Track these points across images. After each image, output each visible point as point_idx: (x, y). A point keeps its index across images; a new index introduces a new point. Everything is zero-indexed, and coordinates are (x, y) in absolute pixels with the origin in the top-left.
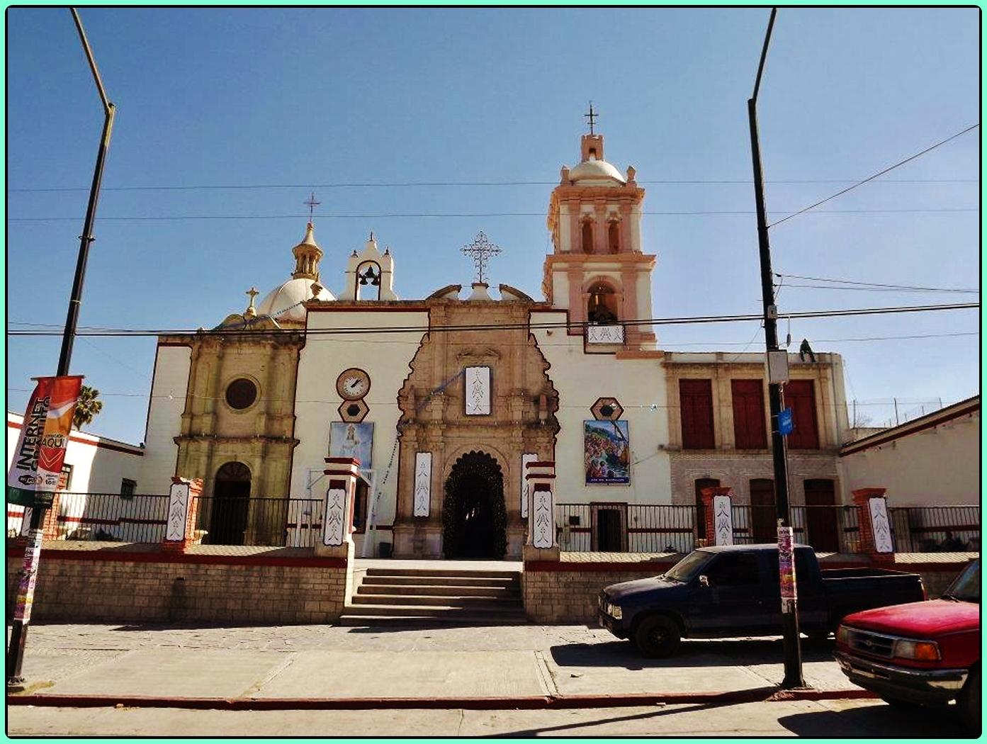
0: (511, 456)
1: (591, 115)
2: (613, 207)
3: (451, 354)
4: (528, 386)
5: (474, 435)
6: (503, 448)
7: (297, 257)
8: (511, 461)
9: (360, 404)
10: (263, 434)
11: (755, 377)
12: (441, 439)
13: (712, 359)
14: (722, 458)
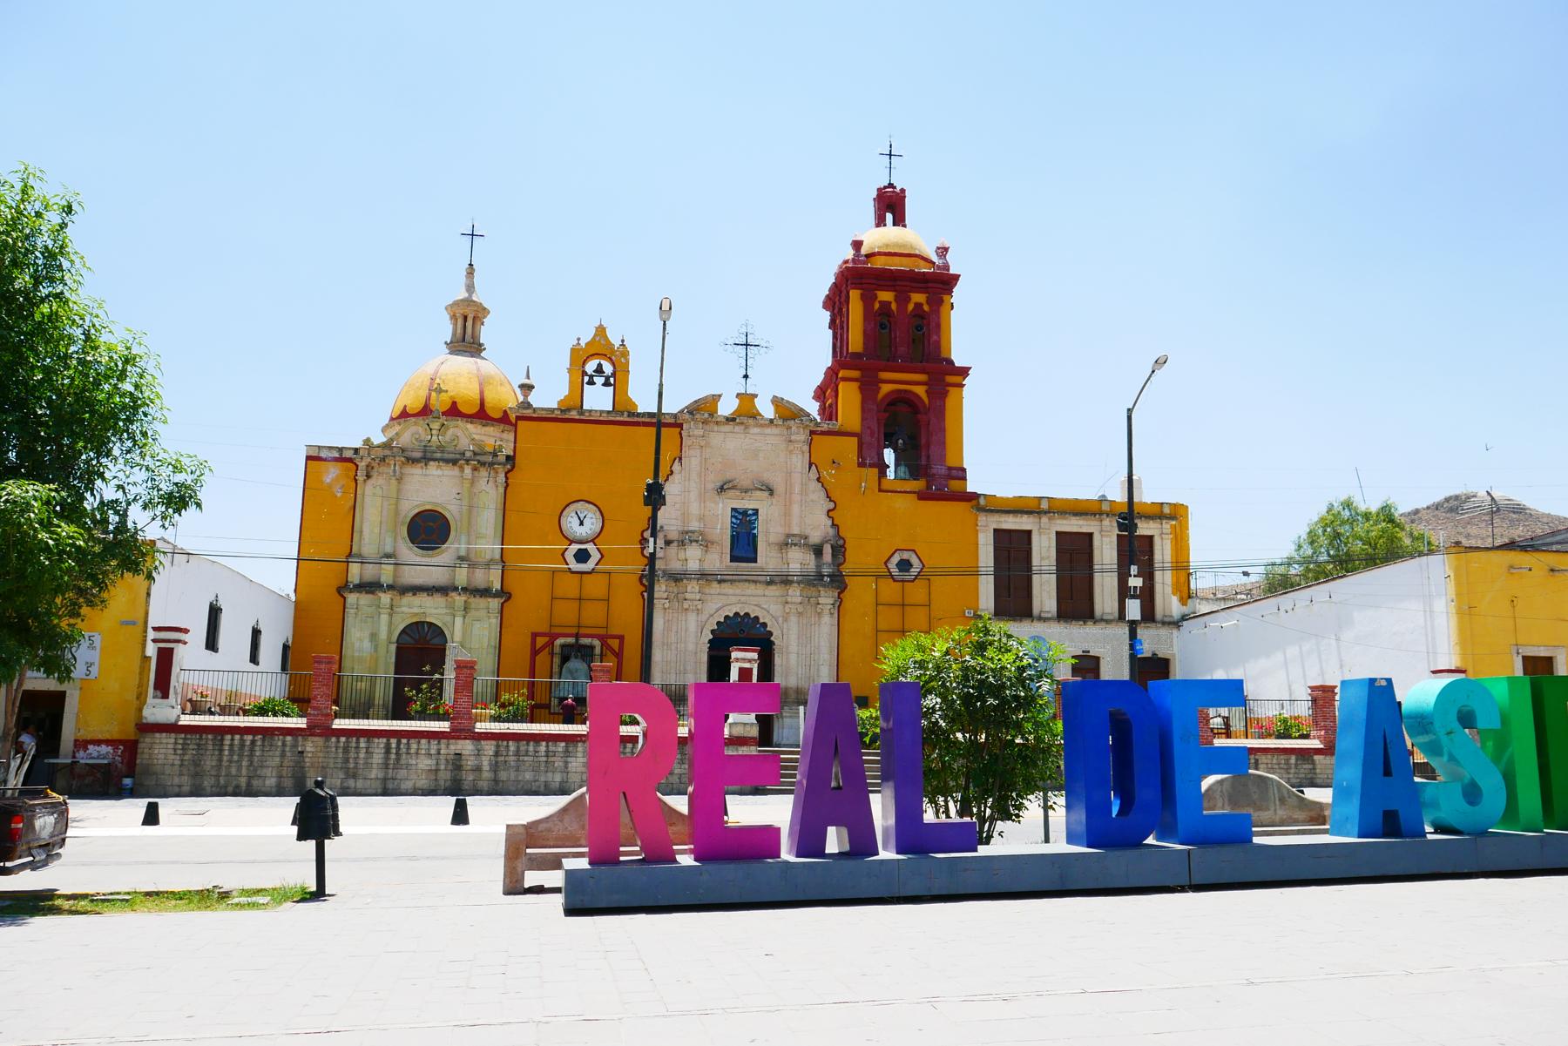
0: (786, 620)
1: (890, 155)
2: (918, 298)
3: (710, 486)
4: (807, 532)
5: (738, 591)
6: (775, 609)
7: (454, 317)
8: (785, 626)
9: (590, 547)
11: (1084, 530)
12: (698, 597)
13: (1033, 505)
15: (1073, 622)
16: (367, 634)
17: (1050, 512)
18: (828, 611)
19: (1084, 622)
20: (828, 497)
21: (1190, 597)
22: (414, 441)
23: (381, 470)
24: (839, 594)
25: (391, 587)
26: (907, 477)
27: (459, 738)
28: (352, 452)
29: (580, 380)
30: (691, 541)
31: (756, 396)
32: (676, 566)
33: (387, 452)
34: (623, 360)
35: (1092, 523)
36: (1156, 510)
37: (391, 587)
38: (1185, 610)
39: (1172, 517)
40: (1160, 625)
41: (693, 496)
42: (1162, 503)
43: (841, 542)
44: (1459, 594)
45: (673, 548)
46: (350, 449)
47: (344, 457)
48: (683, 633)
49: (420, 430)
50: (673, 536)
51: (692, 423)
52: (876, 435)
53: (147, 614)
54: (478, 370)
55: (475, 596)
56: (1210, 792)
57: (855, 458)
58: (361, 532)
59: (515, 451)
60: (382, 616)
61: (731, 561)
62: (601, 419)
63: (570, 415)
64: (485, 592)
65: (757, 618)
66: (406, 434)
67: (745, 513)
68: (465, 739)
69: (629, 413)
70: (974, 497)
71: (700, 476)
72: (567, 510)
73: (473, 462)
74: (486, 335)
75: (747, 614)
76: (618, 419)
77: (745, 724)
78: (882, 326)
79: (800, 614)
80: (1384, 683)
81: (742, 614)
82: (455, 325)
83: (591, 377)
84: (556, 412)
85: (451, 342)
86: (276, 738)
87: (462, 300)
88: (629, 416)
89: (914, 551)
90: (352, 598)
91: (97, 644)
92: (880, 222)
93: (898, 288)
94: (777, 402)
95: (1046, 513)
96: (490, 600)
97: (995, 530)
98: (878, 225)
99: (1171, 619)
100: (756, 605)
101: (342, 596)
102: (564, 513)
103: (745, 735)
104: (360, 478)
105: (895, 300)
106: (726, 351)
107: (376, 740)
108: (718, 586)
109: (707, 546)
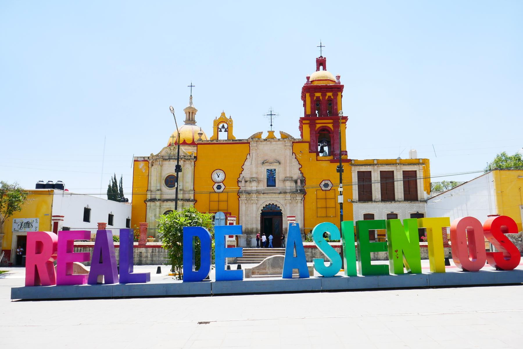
0: (286, 205)
1: (321, 46)
2: (329, 94)
3: (259, 162)
4: (292, 176)
5: (270, 197)
6: (282, 202)
7: (186, 113)
9: (221, 184)
10: (182, 198)
12: (256, 199)
13: (371, 162)
14: (374, 204)
15: (387, 202)
16: (153, 215)
17: (377, 164)
18: (300, 202)
19: (391, 202)
20: (299, 164)
21: (431, 192)
22: (166, 154)
23: (156, 163)
24: (304, 196)
25: (159, 200)
27: (141, 247)
28: (148, 158)
29: (217, 131)
30: (253, 181)
31: (274, 132)
32: (248, 189)
33: (158, 157)
34: (230, 123)
35: (393, 167)
36: (417, 162)
37: (159, 200)
38: (429, 196)
39: (423, 164)
40: (419, 202)
41: (254, 165)
42: (419, 159)
43: (304, 179)
44: (497, 188)
45: (248, 183)
46: (147, 157)
47: (145, 160)
48: (252, 211)
49: (168, 150)
50: (248, 179)
51: (253, 142)
52: (315, 142)
53: (52, 212)
54: (193, 129)
55: (185, 202)
56: (265, 263)
57: (308, 150)
58: (151, 183)
59: (197, 155)
60: (157, 209)
61: (267, 187)
62: (224, 142)
63: (215, 142)
64: (188, 200)
65: (276, 205)
66: (163, 152)
67: (271, 171)
68: (143, 247)
69: (232, 140)
70: (350, 160)
71: (256, 159)
72: (214, 173)
73: (183, 159)
74: (197, 118)
75: (273, 204)
76: (229, 142)
77: (231, 241)
78: (317, 105)
79: (290, 203)
80: (295, 225)
81: (271, 204)
82: (186, 115)
83: (221, 129)
84: (209, 141)
85: (185, 121)
86: (87, 248)
87: (188, 107)
88: (232, 141)
89: (329, 180)
90: (148, 204)
91: (38, 221)
92: (318, 69)
93: (322, 91)
94: (281, 133)
95: (376, 165)
96: (190, 202)
97: (358, 171)
98: (317, 71)
99: (424, 200)
100: (276, 201)
101: (145, 203)
102: (213, 174)
103: (231, 245)
104: (150, 166)
105: (321, 96)
106: (265, 117)
107: (116, 248)
108: (263, 195)
109: (259, 182)
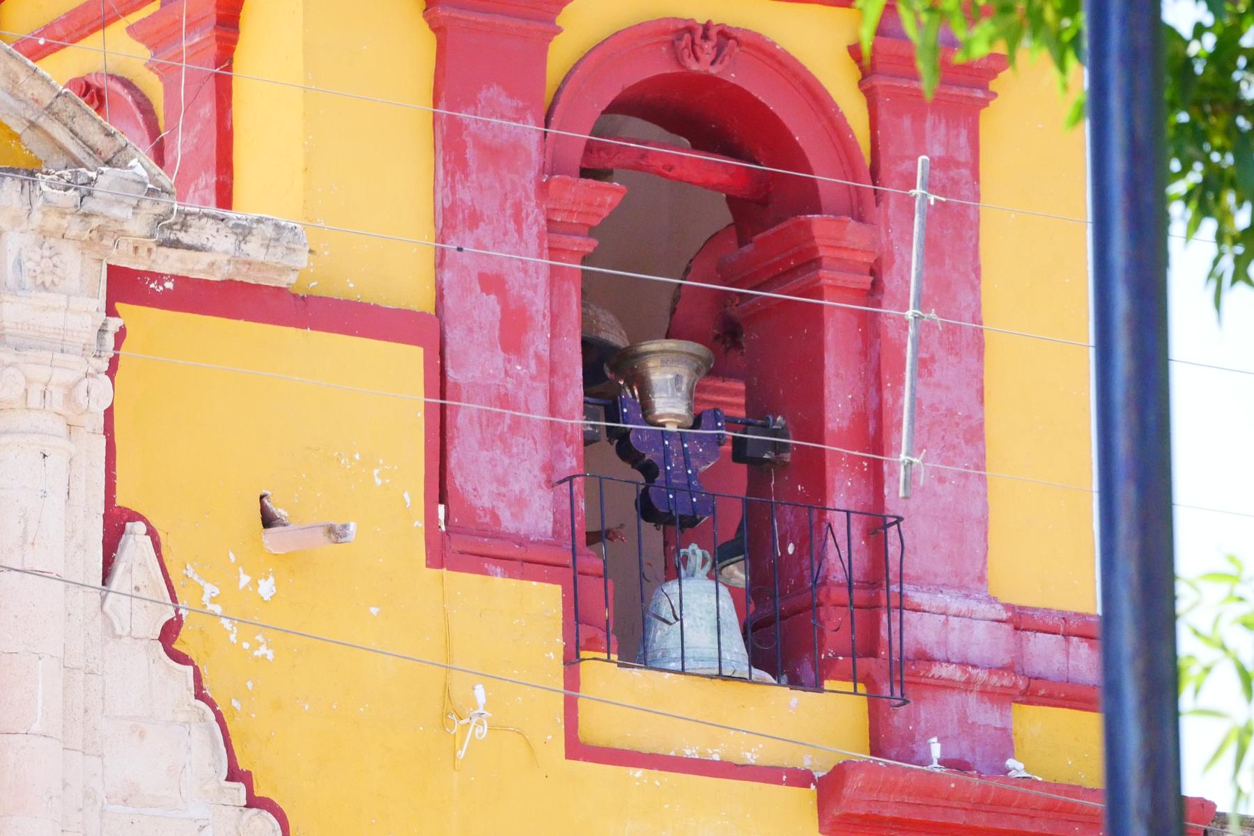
20: (235, 774)
26: (743, 669)
